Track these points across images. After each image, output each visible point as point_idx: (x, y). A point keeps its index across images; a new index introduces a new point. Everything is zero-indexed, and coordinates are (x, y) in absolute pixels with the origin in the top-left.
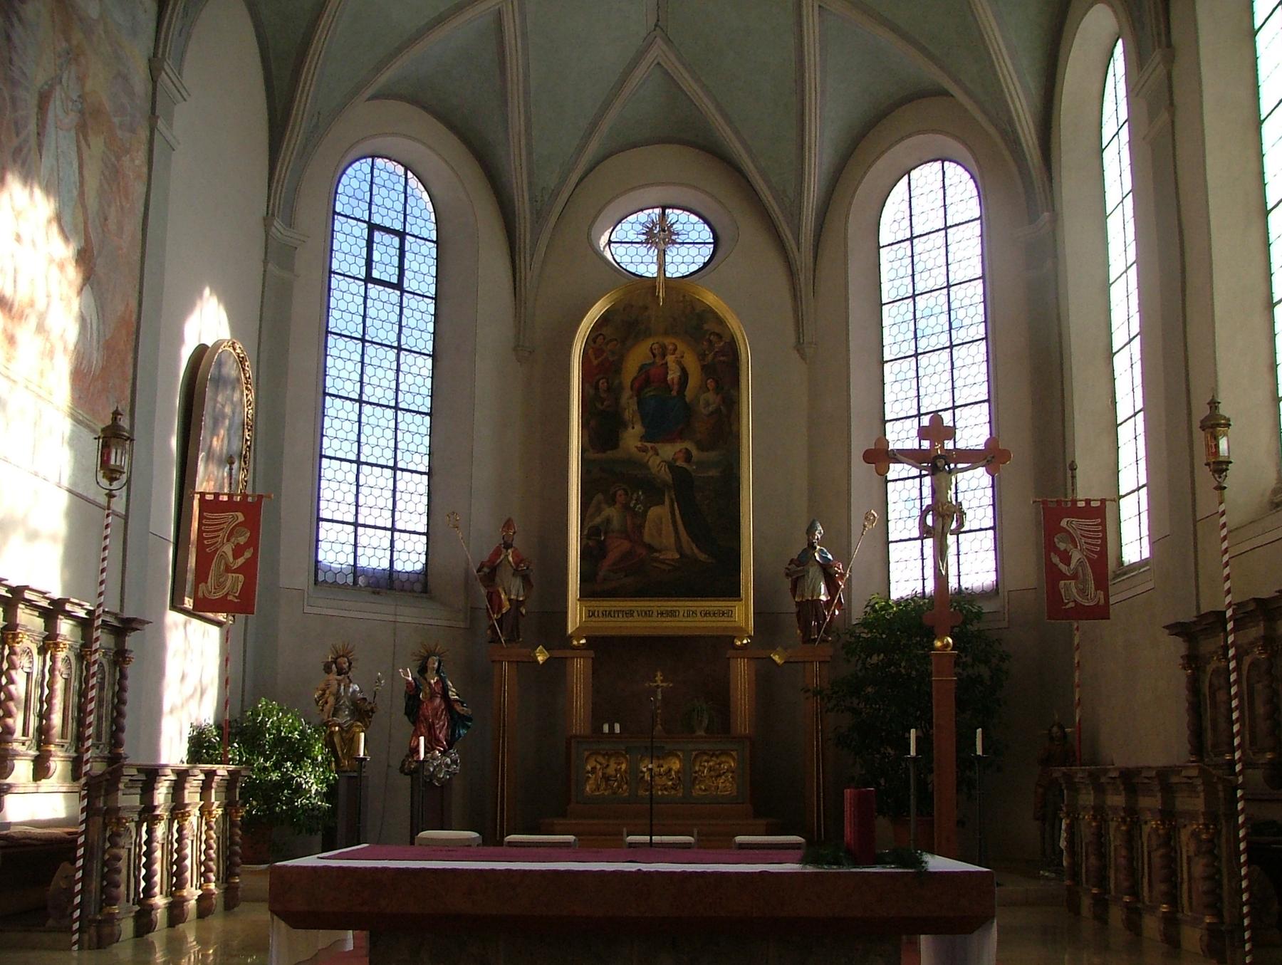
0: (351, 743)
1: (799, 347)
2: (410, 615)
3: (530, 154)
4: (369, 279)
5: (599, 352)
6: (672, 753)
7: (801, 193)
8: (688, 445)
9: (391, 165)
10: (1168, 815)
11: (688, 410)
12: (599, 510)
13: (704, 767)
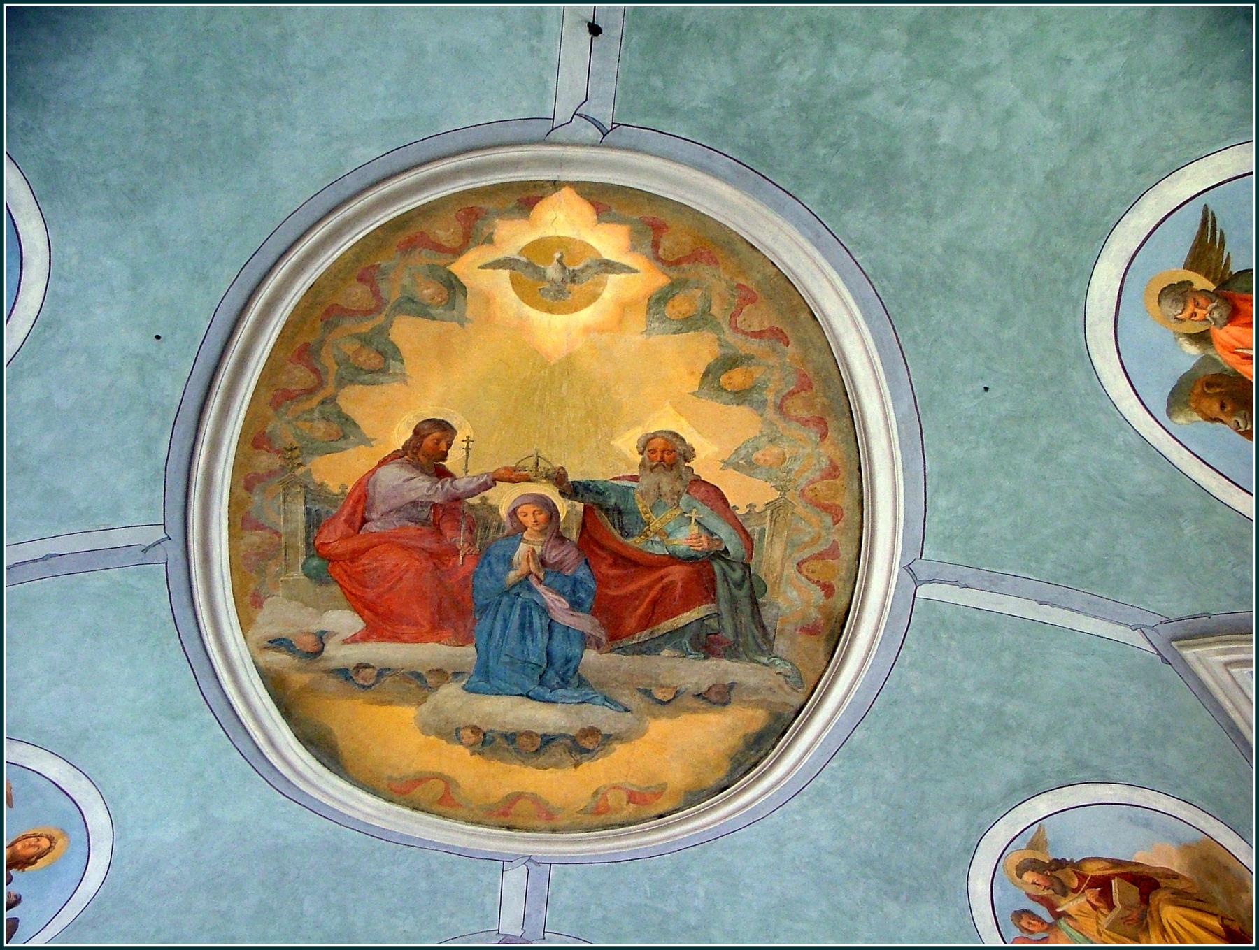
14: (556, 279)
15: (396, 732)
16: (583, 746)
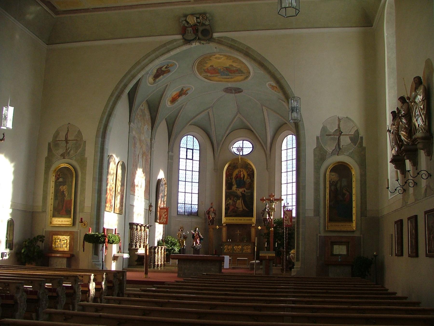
0: (183, 243)
1: (267, 168)
2: (195, 220)
3: (216, 134)
5: (229, 172)
6: (239, 245)
7: (267, 140)
8: (245, 189)
9: (191, 136)
11: (245, 182)
12: (228, 201)
13: (245, 248)
15: (216, 78)
16: (231, 78)
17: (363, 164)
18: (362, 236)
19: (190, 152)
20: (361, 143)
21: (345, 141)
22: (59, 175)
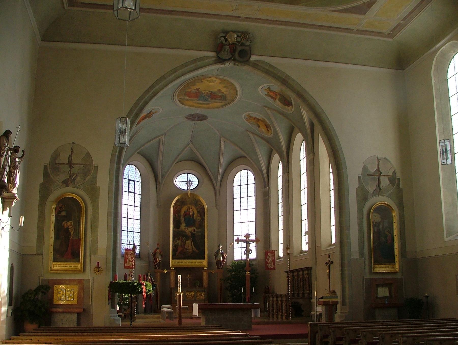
1: (216, 206)
3: (162, 164)
4: (129, 192)
5: (176, 208)
6: (192, 291)
8: (195, 228)
10: (282, 301)
11: (194, 221)
12: (176, 241)
14: (212, 81)
15: (191, 103)
17: (401, 206)
18: (403, 277)
19: (132, 183)
20: (399, 184)
21: (385, 182)
22: (61, 208)
